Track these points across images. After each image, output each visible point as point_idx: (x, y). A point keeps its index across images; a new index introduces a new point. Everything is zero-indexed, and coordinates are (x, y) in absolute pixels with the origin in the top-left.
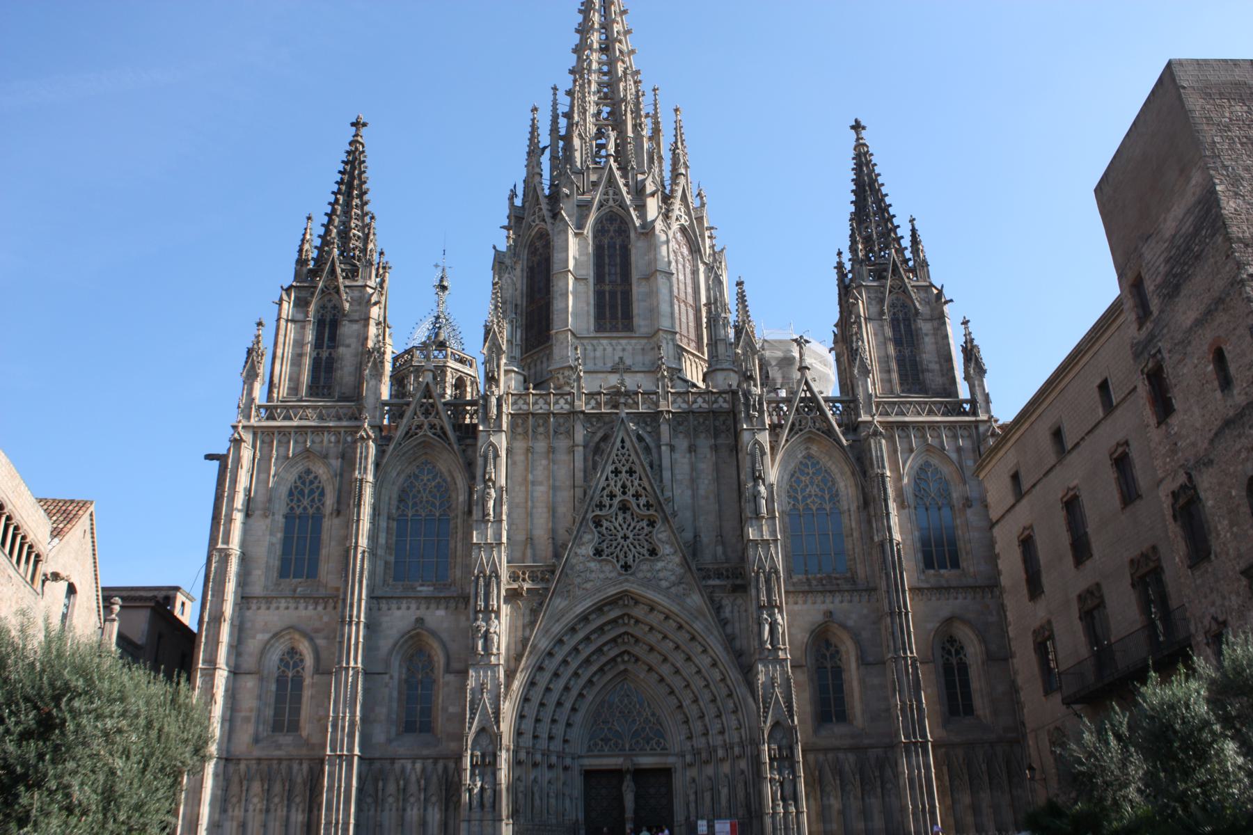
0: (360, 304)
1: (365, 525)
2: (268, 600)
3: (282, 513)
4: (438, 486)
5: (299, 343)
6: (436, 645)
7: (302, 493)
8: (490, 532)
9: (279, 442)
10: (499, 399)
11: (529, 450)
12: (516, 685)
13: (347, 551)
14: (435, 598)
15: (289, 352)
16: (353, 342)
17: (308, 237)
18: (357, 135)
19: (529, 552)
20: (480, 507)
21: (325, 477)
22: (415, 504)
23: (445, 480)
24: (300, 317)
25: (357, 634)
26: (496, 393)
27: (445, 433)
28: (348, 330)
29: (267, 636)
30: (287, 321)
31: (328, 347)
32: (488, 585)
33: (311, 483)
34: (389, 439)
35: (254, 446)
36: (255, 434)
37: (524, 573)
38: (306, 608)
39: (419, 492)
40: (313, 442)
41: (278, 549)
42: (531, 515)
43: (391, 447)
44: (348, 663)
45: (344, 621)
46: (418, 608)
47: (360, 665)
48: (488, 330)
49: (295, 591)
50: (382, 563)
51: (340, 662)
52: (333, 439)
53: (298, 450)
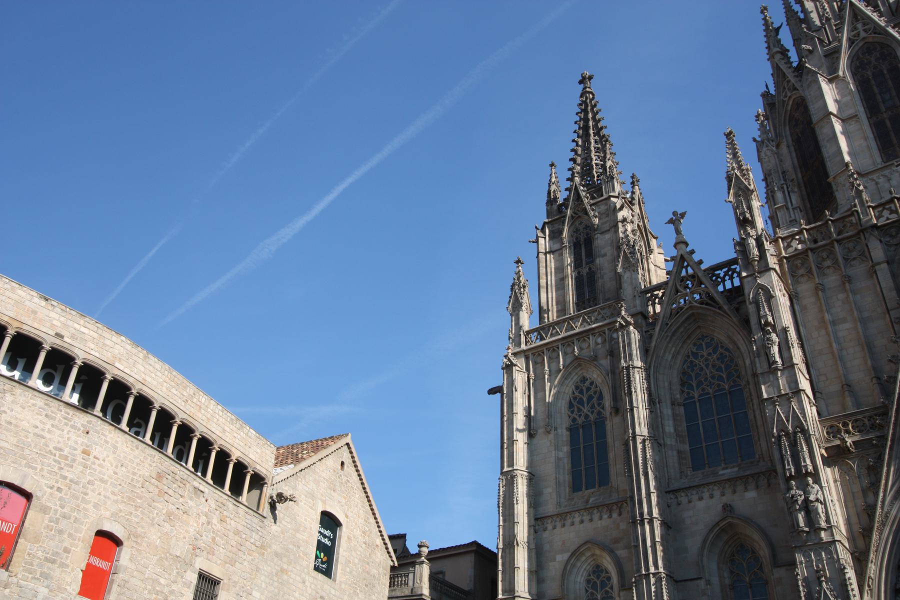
0: (608, 215)
1: (641, 413)
2: (562, 516)
3: (564, 426)
4: (721, 358)
5: (560, 269)
6: (756, 536)
7: (581, 402)
8: (782, 382)
9: (550, 359)
10: (759, 241)
11: (819, 288)
12: (872, 569)
13: (626, 444)
14: (741, 478)
15: (552, 279)
16: (609, 251)
17: (553, 180)
18: (585, 88)
19: (849, 401)
20: (763, 358)
21: (600, 380)
22: (700, 384)
23: (727, 350)
24: (557, 246)
25: (653, 533)
26: (753, 233)
27: (712, 298)
28: (601, 241)
29: (566, 556)
30: (545, 254)
31: (587, 263)
32: (794, 445)
33: (588, 389)
34: (653, 324)
35: (528, 370)
36: (527, 359)
37: (845, 425)
38: (601, 518)
39: (702, 369)
40: (581, 349)
41: (567, 462)
42: (841, 358)
43: (657, 329)
44: (647, 569)
45: (636, 522)
46: (723, 494)
47: (661, 570)
48: (729, 179)
49: (587, 502)
50: (675, 453)
51: (639, 570)
52: (599, 340)
53: (569, 361)
